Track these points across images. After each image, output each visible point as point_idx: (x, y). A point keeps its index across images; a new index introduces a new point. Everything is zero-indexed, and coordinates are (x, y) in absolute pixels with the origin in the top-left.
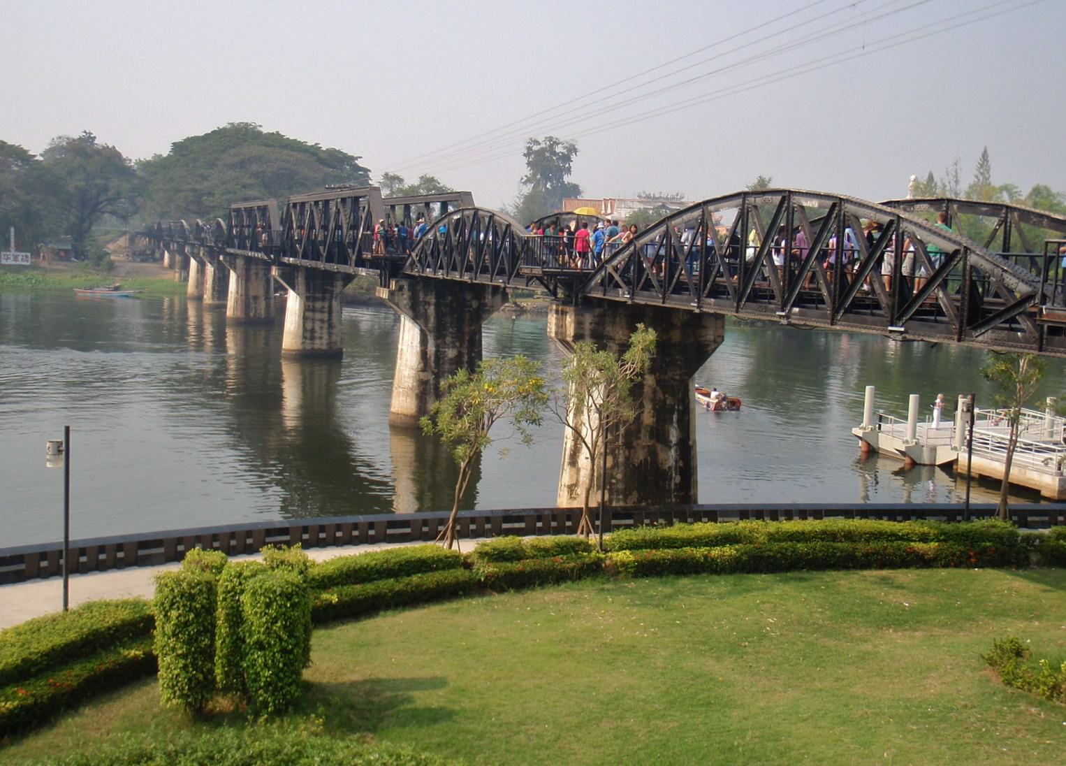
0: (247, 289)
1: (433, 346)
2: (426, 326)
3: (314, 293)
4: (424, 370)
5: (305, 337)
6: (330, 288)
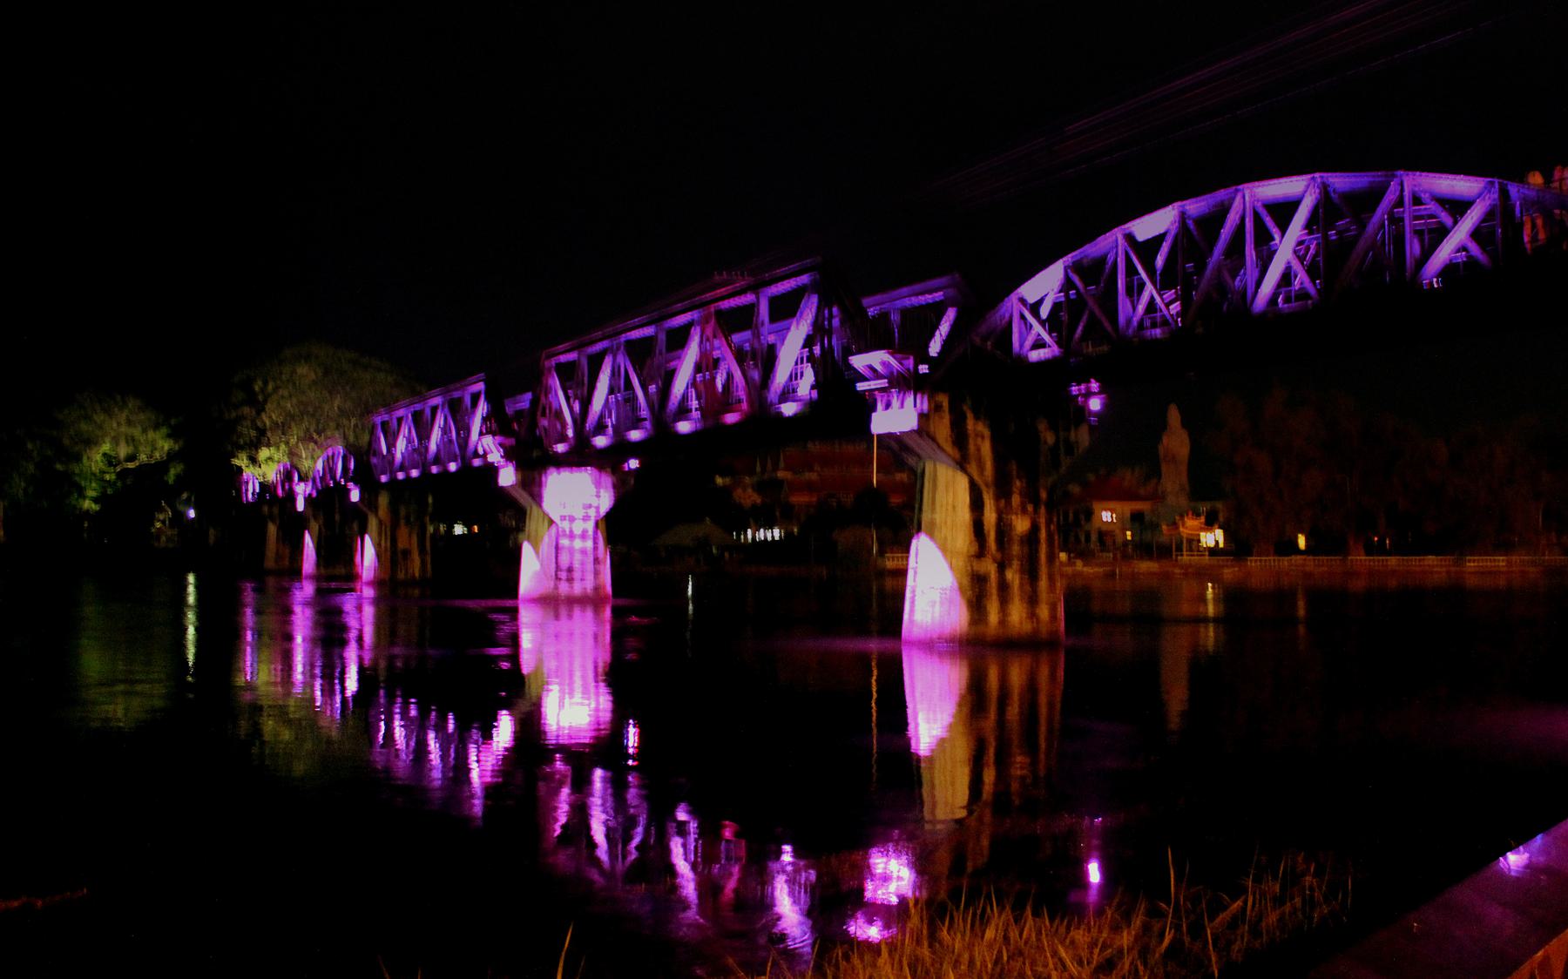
0: (394, 540)
1: (993, 508)
4: (981, 553)
5: (558, 578)
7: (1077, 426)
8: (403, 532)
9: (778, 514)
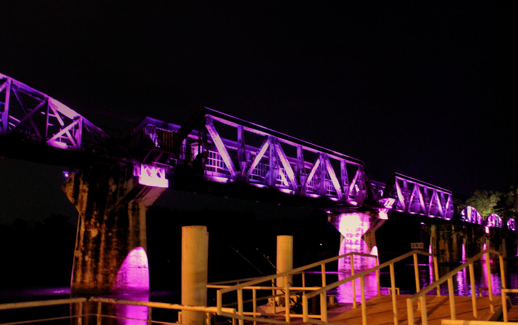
7: (127, 180)
8: (442, 242)
9: (473, 228)
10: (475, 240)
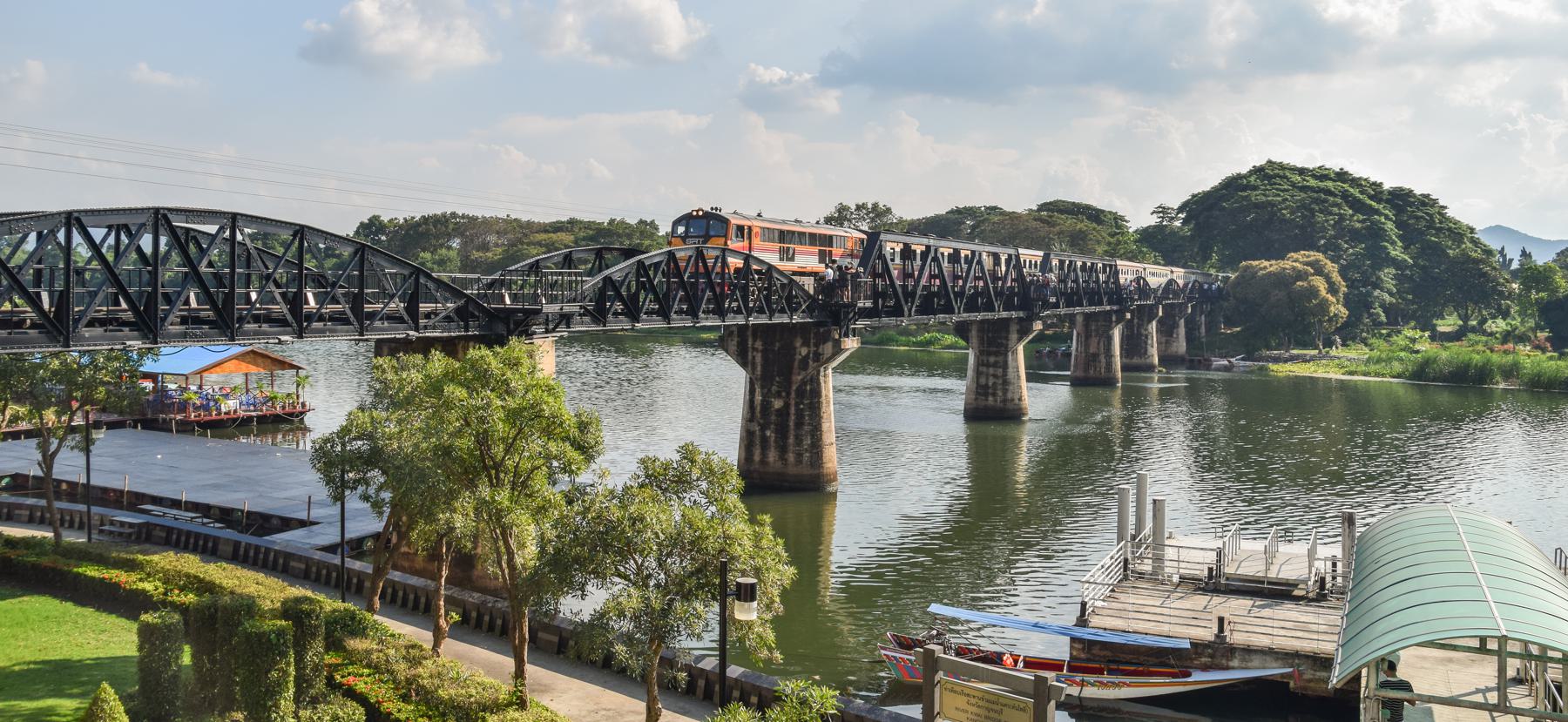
0: (1087, 346)
2: (753, 373)
3: (990, 345)
5: (978, 393)
6: (1004, 342)
8: (1094, 341)
10: (1139, 328)
